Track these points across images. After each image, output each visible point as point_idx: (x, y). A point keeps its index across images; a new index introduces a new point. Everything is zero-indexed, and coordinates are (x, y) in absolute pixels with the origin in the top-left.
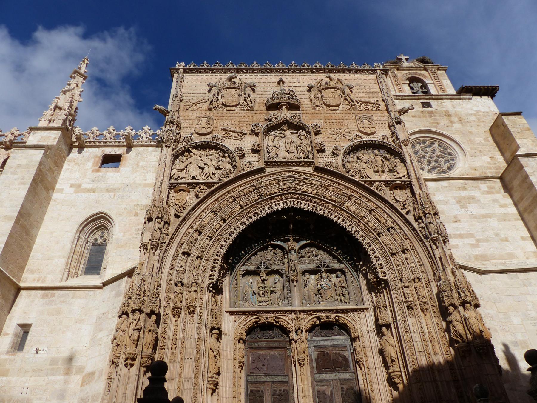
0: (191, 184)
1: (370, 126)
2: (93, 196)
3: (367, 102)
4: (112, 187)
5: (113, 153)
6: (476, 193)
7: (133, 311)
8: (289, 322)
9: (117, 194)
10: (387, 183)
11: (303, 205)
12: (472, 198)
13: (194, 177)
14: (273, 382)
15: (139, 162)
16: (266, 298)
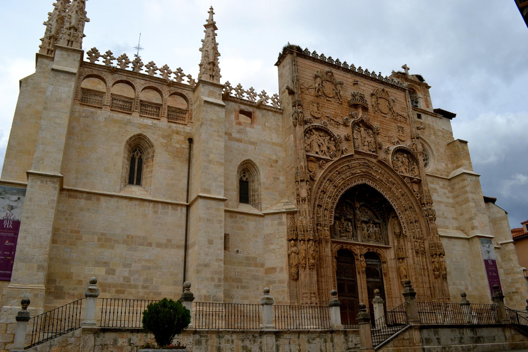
0: (316, 158)
1: (403, 135)
2: (242, 145)
3: (401, 115)
4: (252, 140)
5: (246, 110)
6: (437, 187)
7: (309, 240)
8: (357, 251)
9: (257, 147)
10: (411, 179)
11: (370, 183)
12: (435, 189)
13: (317, 153)
14: (348, 280)
15: (265, 123)
16: (344, 235)
